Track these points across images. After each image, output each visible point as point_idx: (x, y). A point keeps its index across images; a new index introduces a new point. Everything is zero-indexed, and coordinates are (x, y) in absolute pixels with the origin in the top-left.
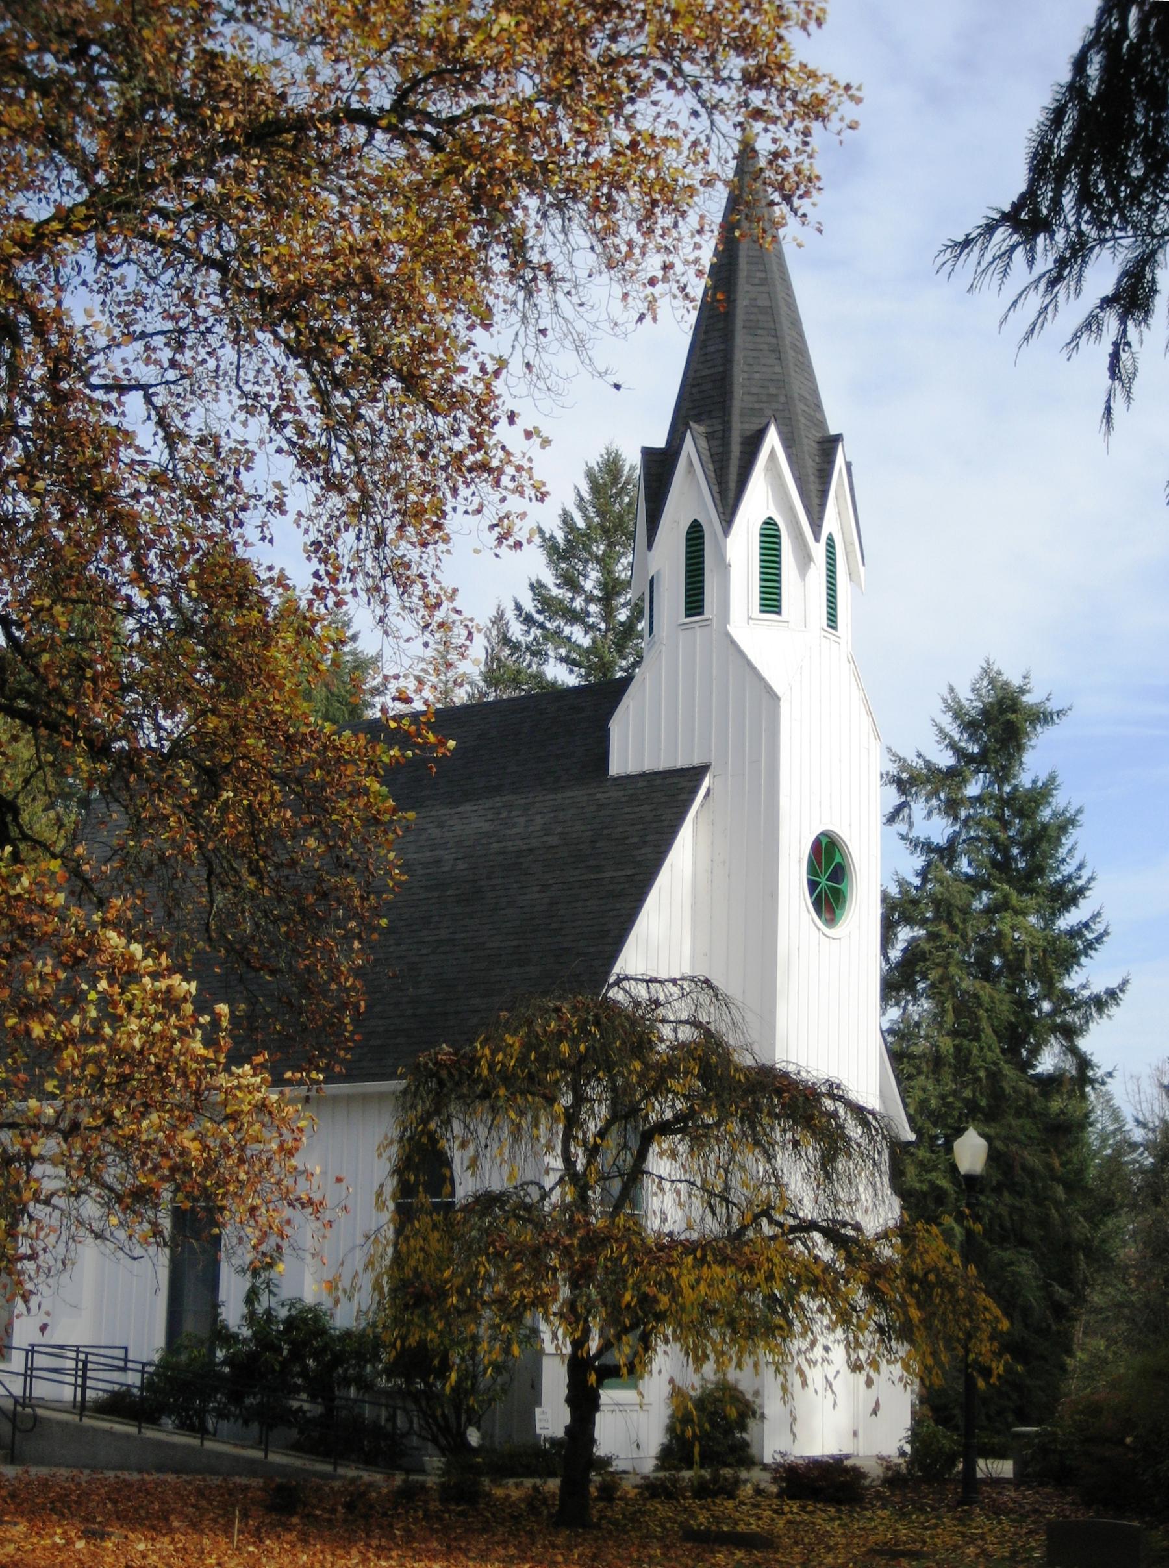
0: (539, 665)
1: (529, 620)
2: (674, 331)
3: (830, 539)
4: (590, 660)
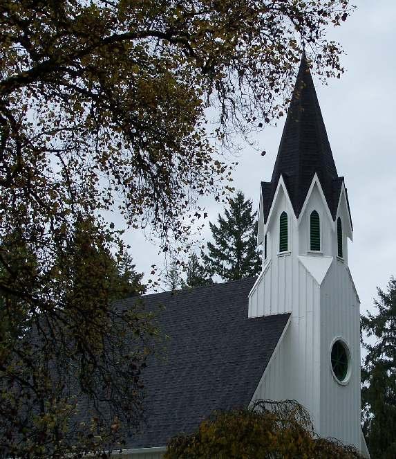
0: (211, 276)
1: (206, 258)
2: (271, 137)
3: (339, 219)
4: (234, 275)
